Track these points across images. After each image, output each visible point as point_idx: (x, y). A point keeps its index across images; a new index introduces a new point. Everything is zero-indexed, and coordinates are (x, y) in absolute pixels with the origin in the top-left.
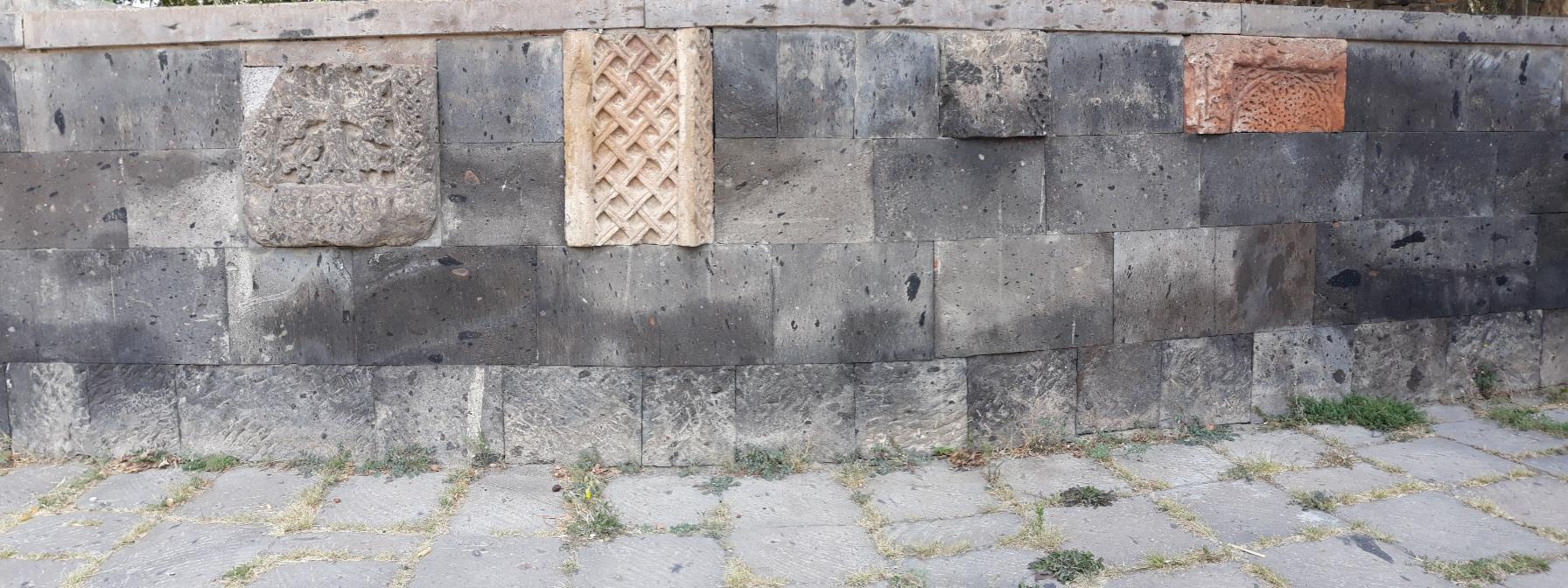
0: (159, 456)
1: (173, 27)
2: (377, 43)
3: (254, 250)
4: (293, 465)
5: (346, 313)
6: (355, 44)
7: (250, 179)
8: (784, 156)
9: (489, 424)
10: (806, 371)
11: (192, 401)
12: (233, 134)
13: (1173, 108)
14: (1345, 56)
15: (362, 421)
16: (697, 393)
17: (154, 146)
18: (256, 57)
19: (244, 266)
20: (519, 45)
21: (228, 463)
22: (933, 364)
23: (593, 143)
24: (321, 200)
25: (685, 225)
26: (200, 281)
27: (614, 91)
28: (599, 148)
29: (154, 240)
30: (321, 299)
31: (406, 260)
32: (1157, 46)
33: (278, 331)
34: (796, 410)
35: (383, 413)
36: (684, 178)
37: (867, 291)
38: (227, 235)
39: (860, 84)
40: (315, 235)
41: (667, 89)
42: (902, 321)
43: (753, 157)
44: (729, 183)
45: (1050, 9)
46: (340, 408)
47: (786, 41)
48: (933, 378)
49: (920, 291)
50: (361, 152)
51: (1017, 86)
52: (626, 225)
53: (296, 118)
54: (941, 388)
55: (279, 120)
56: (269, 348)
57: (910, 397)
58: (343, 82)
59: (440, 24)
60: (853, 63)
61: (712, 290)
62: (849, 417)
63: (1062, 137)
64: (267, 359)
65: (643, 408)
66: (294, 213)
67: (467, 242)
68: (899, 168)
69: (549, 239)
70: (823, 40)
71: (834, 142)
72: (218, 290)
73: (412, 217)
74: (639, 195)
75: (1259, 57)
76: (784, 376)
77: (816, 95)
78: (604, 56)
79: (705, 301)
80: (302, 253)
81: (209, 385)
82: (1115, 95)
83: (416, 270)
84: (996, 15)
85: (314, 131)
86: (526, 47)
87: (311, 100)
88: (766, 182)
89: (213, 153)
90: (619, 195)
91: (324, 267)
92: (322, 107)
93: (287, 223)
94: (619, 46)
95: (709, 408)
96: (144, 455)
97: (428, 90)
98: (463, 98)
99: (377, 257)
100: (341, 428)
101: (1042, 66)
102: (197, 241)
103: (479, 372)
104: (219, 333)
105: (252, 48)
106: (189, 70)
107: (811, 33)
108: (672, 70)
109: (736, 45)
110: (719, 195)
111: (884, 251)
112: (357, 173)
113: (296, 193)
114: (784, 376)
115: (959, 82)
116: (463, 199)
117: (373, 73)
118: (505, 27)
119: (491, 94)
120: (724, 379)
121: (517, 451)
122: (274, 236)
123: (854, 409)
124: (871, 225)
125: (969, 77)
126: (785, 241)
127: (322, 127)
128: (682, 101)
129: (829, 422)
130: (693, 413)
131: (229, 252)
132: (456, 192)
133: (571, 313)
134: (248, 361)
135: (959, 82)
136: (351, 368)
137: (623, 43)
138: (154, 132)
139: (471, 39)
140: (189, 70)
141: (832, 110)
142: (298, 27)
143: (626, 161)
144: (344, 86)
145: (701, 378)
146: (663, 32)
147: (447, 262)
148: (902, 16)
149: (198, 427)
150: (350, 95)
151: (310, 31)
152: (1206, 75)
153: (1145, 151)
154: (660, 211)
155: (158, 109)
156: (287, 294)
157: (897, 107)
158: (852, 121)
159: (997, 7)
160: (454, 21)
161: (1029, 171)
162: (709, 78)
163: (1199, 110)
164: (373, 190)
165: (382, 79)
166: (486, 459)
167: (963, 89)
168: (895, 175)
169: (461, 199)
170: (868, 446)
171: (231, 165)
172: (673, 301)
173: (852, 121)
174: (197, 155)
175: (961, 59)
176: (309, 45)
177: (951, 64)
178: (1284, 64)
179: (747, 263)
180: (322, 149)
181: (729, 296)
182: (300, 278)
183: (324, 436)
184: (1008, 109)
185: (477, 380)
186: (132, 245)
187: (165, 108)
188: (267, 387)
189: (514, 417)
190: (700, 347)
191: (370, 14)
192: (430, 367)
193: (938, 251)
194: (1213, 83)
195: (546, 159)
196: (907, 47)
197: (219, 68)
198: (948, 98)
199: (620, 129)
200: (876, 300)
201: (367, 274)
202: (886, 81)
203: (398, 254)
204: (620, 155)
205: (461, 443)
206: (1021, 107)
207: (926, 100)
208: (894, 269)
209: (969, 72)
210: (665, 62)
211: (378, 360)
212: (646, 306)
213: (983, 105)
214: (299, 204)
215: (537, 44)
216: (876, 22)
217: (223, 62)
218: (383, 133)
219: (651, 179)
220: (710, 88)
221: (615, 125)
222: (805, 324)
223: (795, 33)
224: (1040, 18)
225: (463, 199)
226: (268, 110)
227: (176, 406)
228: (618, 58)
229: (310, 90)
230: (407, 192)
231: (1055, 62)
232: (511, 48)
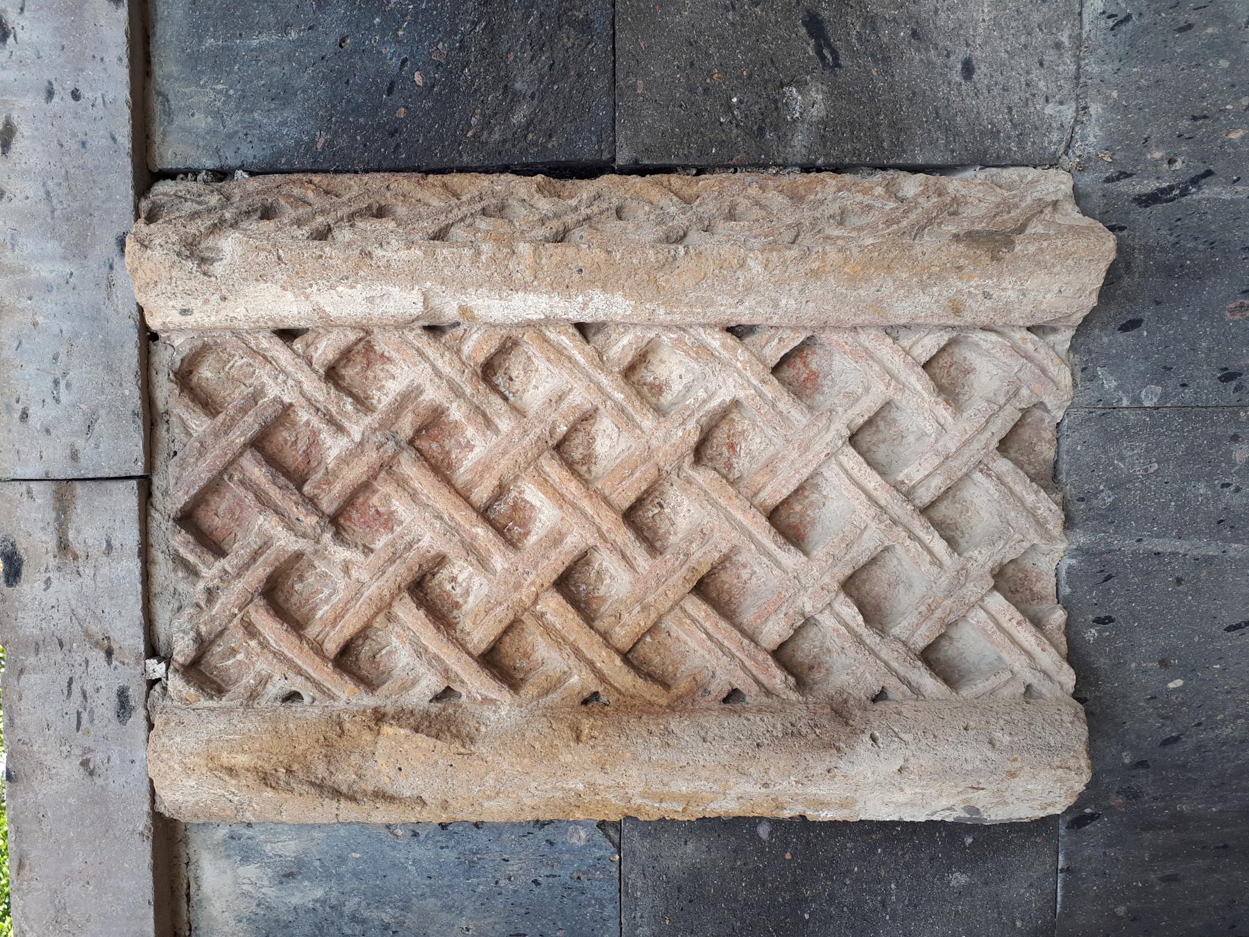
25: (1007, 289)
27: (409, 613)
36: (783, 301)
41: (406, 374)
52: (983, 558)
69: (1025, 886)
74: (847, 505)
90: (850, 585)
108: (325, 349)
109: (219, 62)
128: (449, 310)
137: (210, 571)
143: (703, 557)
146: (165, 389)
154: (919, 409)
162: (355, 187)
195: (687, 895)
199: (567, 583)
204: (679, 582)
210: (289, 381)
219: (781, 444)
220: (404, 183)
221: (553, 605)
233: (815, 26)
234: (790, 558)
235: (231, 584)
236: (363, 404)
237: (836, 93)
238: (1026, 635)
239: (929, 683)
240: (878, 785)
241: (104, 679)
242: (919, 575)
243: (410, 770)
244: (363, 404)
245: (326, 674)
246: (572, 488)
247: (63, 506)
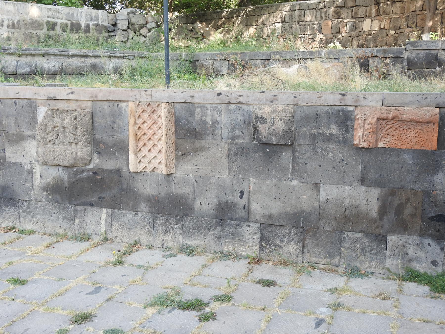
0: (13, 228)
1: (18, 94)
2: (75, 101)
3: (40, 165)
4: (50, 235)
5: (66, 187)
6: (69, 101)
7: (38, 141)
8: (198, 145)
9: (108, 228)
10: (205, 220)
11: (24, 211)
12: (34, 128)
13: (349, 136)
14: (438, 115)
15: (71, 222)
16: (170, 224)
17: (13, 130)
18: (41, 104)
19: (38, 170)
20: (116, 104)
21: (32, 232)
22: (248, 224)
23: (136, 138)
24: (57, 151)
26: (25, 173)
28: (138, 140)
29: (13, 160)
30: (59, 182)
31: (83, 172)
32: (343, 111)
33: (47, 191)
34: (201, 233)
35: (77, 221)
36: (163, 151)
37: (226, 194)
38: (33, 160)
39: (224, 122)
40: (55, 162)
42: (237, 207)
43: (188, 145)
44: (180, 153)
45: (295, 97)
46: (64, 218)
47: (198, 107)
48: (248, 228)
49: (244, 196)
50: (69, 137)
51: (280, 126)
52: (147, 165)
54: (251, 232)
56: (45, 197)
57: (239, 235)
58: (65, 114)
59: (92, 97)
60: (221, 115)
61: (175, 190)
62: (219, 238)
63: (300, 145)
64: (44, 200)
65: (153, 227)
67: (100, 167)
68: (238, 152)
69: (125, 168)
70: (211, 107)
71: (214, 142)
72: (31, 177)
73: (82, 159)
75: (390, 116)
76: (198, 221)
77: (208, 126)
78: (140, 110)
79: (173, 193)
80: (54, 167)
81: (28, 207)
82: (323, 130)
83: (86, 175)
84: (274, 99)
85: (56, 129)
86: (118, 105)
88: (192, 154)
89: (29, 133)
91: (60, 172)
92: (57, 121)
93: (48, 158)
94: (145, 107)
95: (175, 229)
96: (9, 228)
97: (88, 118)
98: (100, 121)
99: (75, 170)
100: (65, 224)
101: (291, 118)
102: (25, 161)
103: (104, 210)
104: (31, 191)
105: (40, 101)
106: (23, 107)
107: (207, 105)
109: (182, 108)
110: (177, 157)
111: (232, 180)
112: (68, 143)
113: (50, 148)
114: (198, 221)
115: (259, 123)
116: (100, 153)
117: (72, 112)
118: (111, 99)
119: (108, 120)
120: (179, 220)
121: (116, 237)
123: (220, 236)
124: (227, 171)
125: (262, 122)
126: (198, 174)
127: (58, 128)
129: (212, 239)
130: (169, 231)
131: (34, 165)
132: (98, 150)
133: (132, 193)
134: (39, 200)
135: (259, 123)
136: (68, 205)
137: (146, 106)
138: (13, 125)
139: (102, 102)
140: (23, 107)
141: (214, 131)
142: (52, 96)
145: (172, 219)
146: (159, 103)
147: (95, 173)
148: (239, 100)
149: (25, 220)
151: (56, 97)
152: (364, 123)
153: (335, 152)
154: (158, 161)
155: (14, 119)
156: (49, 180)
157: (237, 131)
158: (221, 135)
159: (275, 96)
160: (96, 96)
161: (286, 157)
163: (360, 137)
164: (72, 149)
165: (75, 113)
166: (106, 239)
167: (260, 126)
168: (236, 154)
169: (99, 153)
170: (226, 250)
171: (34, 138)
172: (163, 192)
173: (221, 135)
174: (25, 134)
175: (260, 115)
177: (257, 117)
178: (403, 119)
179: (185, 181)
180: (58, 135)
181: (180, 192)
182: (53, 175)
183: (60, 227)
184: (277, 134)
185: (104, 213)
186: (7, 161)
187: (16, 118)
188: (44, 209)
189: (115, 227)
190: (172, 208)
191: (72, 93)
192: (90, 207)
193: (251, 183)
194: (367, 126)
195: (124, 142)
196: (241, 110)
197: (31, 107)
198: (256, 129)
200: (229, 198)
201: (72, 175)
202: (234, 122)
203: (81, 170)
205: (99, 233)
206: (281, 134)
207: (248, 129)
208: (235, 188)
209: (263, 120)
211: (75, 203)
212: (155, 193)
213: (267, 132)
215: (121, 105)
216: (229, 102)
217: (32, 105)
218: (75, 131)
221: (143, 132)
222: (205, 204)
223: (202, 105)
224: (291, 100)
225: (100, 153)
227: (19, 213)
228: (144, 110)
229: (55, 116)
230: (81, 151)
231: (298, 116)
232: (113, 105)
233: (185, 154)
234: (147, 151)
235: (145, 107)
236: (158, 118)
237: (180, 156)
238: (142, 168)
239: (138, 161)
240: (131, 156)
241: (138, 98)
242: (147, 160)
243: (132, 121)
244: (158, 118)
245: (138, 115)
246: (152, 134)
247: (150, 95)
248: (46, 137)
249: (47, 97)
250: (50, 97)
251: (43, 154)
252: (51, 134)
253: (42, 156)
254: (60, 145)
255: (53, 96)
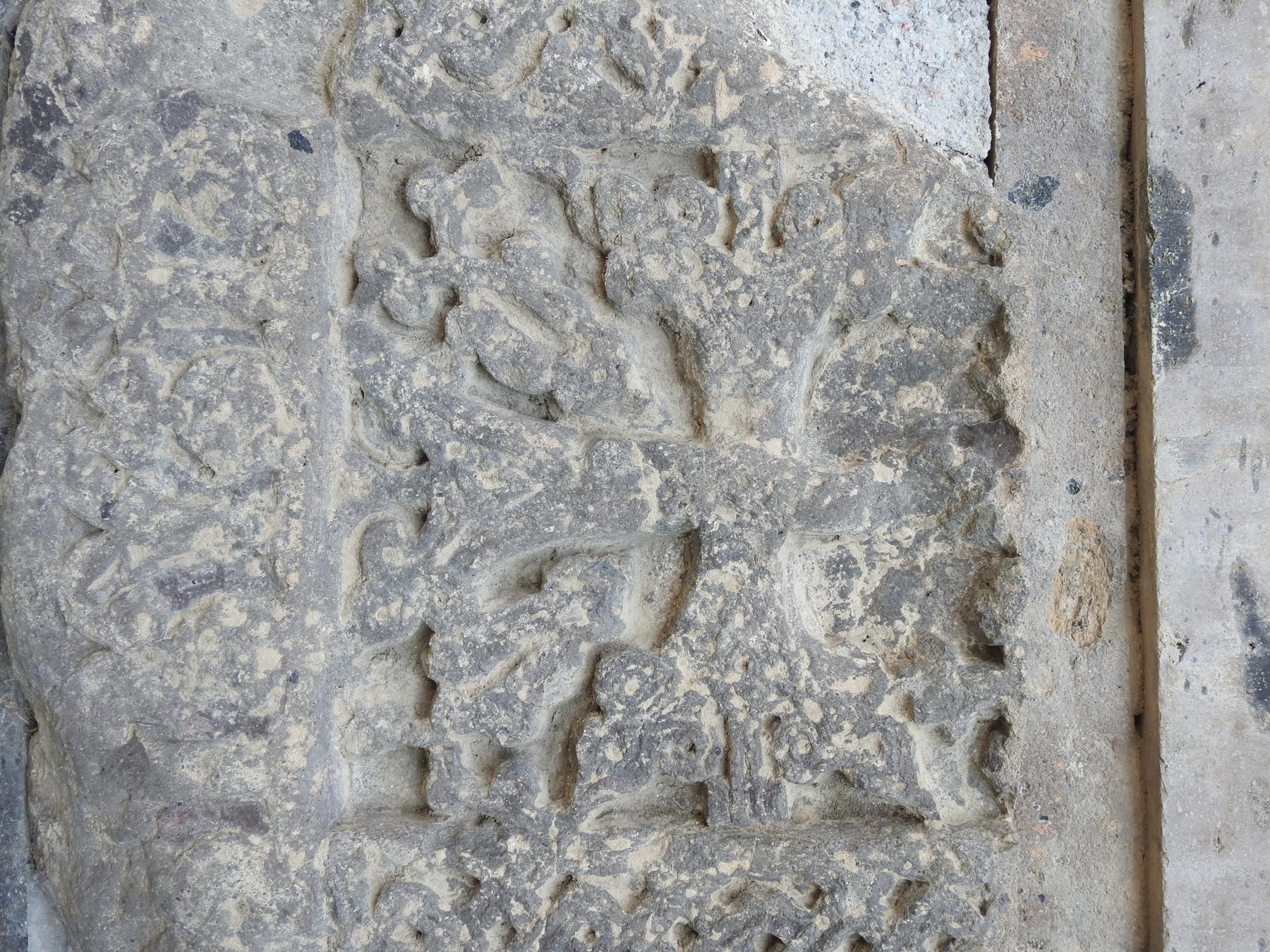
2: (1113, 704)
24: (251, 402)
50: (527, 640)
53: (717, 270)
55: (708, 166)
66: (174, 240)
85: (642, 363)
87: (821, 345)
93: (117, 195)
117: (968, 726)
122: (44, 114)
142: (1211, 278)
144: (888, 528)
150: (841, 567)
151: (1183, 347)
165: (936, 772)
176: (1104, 327)
180: (546, 407)
214: (228, 267)
226: (761, 106)
229: (873, 342)
248: (494, 144)
249: (1187, 178)
250: (1178, 233)
251: (170, 76)
252: (549, 241)
253: (136, 58)
254: (369, 434)
255: (1202, 289)
